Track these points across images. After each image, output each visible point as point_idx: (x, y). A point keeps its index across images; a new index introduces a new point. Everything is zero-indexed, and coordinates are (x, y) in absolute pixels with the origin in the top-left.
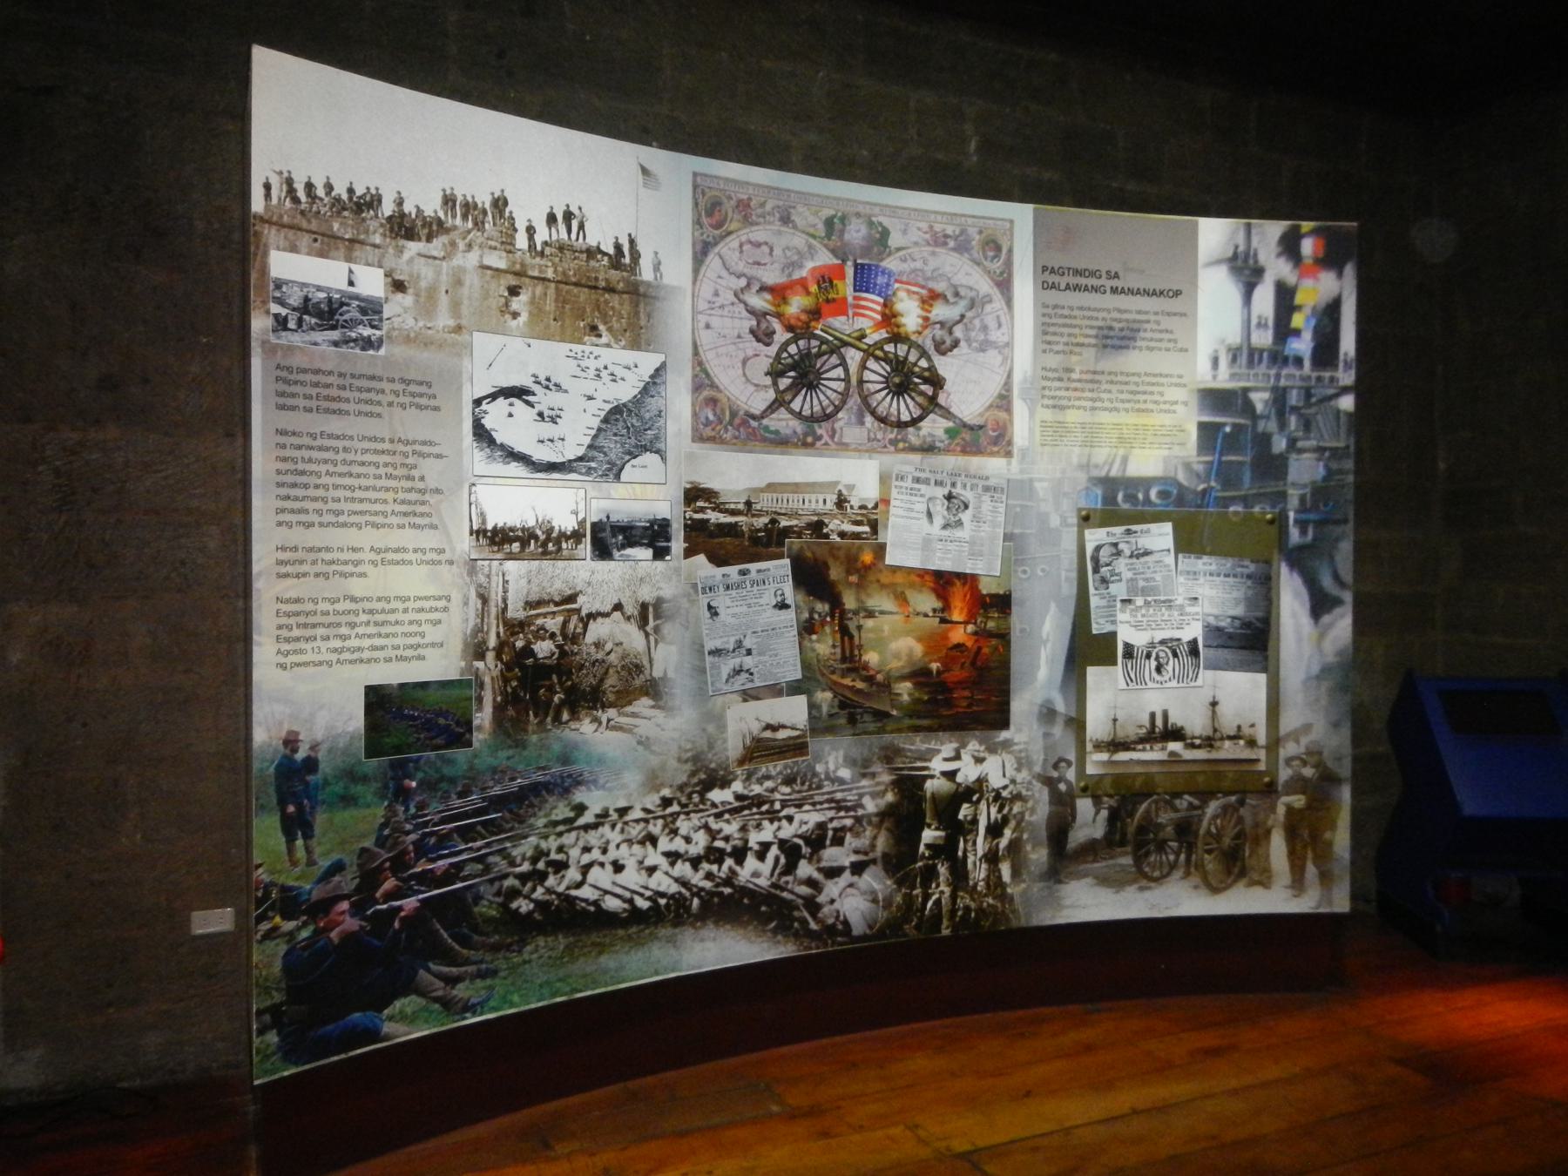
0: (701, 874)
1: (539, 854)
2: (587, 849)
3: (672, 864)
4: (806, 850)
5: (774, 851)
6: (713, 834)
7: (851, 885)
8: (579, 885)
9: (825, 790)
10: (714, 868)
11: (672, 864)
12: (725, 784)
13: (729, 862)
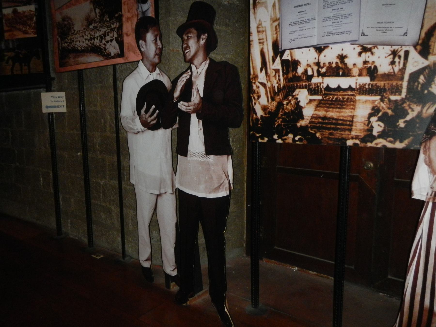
0: (89, 43)
1: (71, 39)
2: (76, 38)
3: (86, 41)
4: (103, 37)
5: (99, 38)
6: (91, 34)
7: (111, 45)
8: (75, 45)
9: (106, 23)
10: (91, 41)
11: (86, 41)
12: (91, 24)
13: (93, 40)
